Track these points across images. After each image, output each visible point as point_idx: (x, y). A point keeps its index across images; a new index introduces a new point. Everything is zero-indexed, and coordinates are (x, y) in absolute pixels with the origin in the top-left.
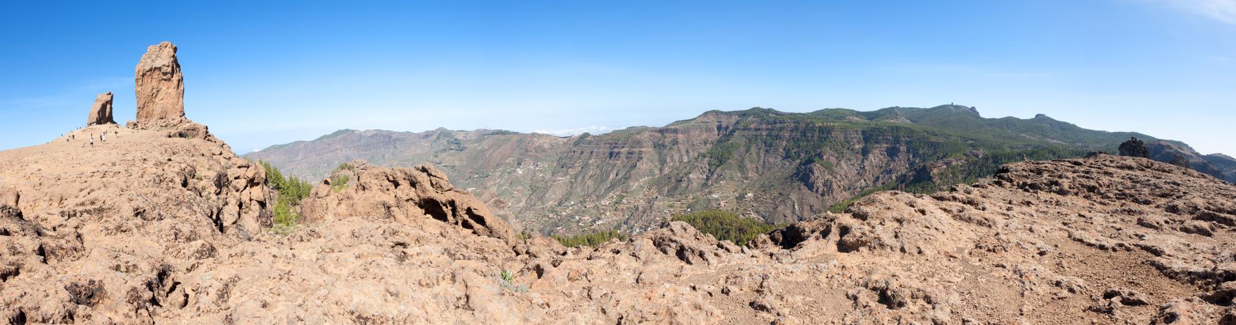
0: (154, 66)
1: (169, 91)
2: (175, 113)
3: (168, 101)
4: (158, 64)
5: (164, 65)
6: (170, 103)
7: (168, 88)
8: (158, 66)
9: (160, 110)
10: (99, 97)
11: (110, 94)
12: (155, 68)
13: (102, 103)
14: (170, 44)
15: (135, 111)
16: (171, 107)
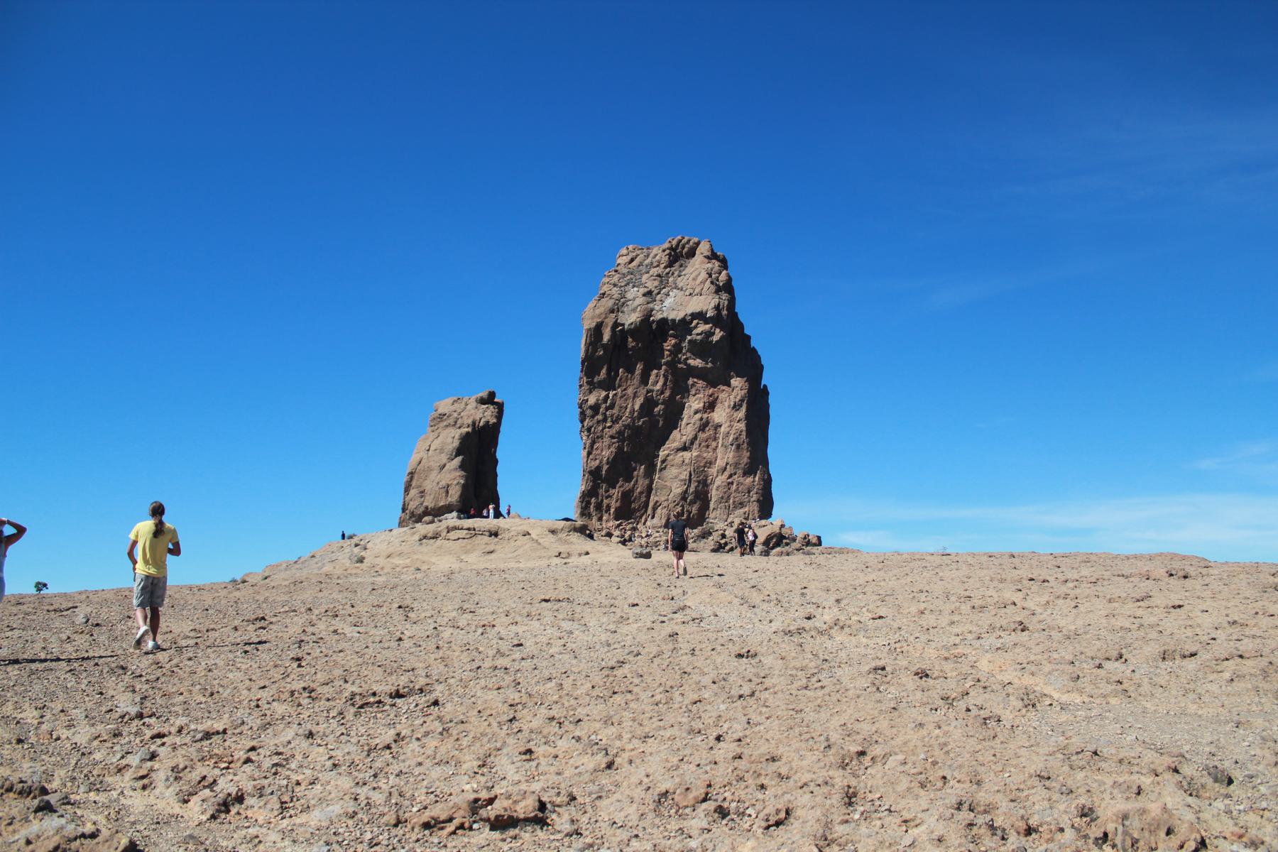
0: (658, 316)
1: (719, 415)
2: (742, 505)
3: (708, 455)
4: (673, 306)
5: (700, 316)
6: (720, 463)
7: (711, 406)
8: (677, 315)
9: (677, 489)
10: (445, 406)
11: (490, 399)
12: (664, 321)
13: (470, 429)
14: (704, 248)
15: (577, 485)
16: (720, 480)
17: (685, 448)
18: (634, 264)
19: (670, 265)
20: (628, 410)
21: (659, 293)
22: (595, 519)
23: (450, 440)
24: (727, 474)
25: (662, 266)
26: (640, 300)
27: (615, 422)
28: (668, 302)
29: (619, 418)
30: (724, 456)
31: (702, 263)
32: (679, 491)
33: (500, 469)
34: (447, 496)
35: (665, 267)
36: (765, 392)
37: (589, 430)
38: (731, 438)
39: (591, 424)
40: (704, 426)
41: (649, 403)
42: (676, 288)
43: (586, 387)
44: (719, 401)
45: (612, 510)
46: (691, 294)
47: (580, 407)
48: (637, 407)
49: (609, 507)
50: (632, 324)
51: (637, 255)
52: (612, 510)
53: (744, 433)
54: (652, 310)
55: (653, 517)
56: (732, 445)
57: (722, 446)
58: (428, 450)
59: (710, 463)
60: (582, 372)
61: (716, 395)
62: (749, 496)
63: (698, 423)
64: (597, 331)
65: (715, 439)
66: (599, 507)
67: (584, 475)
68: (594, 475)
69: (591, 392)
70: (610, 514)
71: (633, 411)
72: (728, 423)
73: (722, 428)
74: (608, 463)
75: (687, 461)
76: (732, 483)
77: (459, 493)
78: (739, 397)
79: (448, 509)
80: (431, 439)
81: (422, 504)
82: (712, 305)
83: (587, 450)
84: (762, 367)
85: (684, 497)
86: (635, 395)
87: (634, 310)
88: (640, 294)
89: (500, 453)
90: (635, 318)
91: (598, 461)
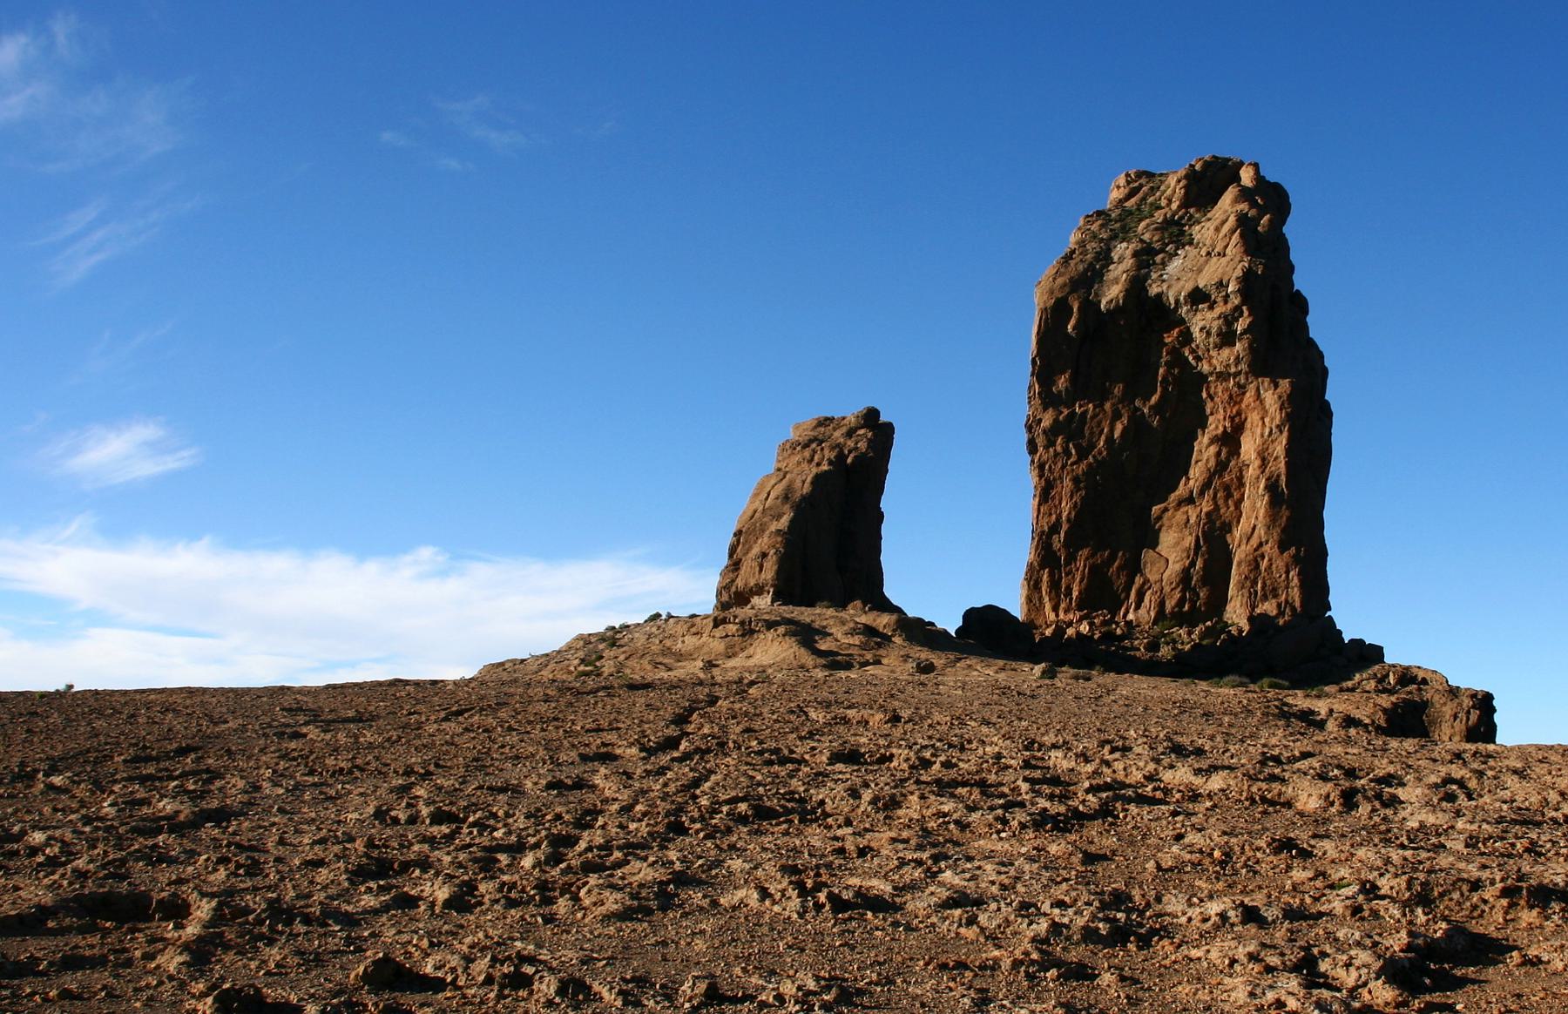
9: (1175, 567)
17: (1190, 500)
18: (1133, 201)
19: (1185, 204)
20: (1103, 437)
21: (1162, 251)
22: (1048, 607)
23: (798, 484)
24: (1254, 542)
25: (1174, 206)
26: (1129, 262)
27: (1082, 455)
28: (1175, 266)
29: (1092, 446)
30: (1254, 509)
31: (1236, 201)
32: (1178, 567)
33: (885, 529)
34: (761, 570)
35: (1180, 208)
36: (1325, 413)
37: (1041, 467)
38: (1262, 486)
39: (1045, 457)
40: (1221, 466)
41: (1137, 425)
42: (1191, 243)
43: (1038, 401)
44: (1248, 425)
45: (1075, 594)
46: (1209, 254)
47: (1029, 428)
48: (1117, 434)
49: (1069, 590)
50: (1112, 300)
51: (1141, 186)
52: (1075, 594)
53: (1283, 478)
54: (1148, 276)
55: (1138, 607)
56: (1264, 495)
57: (1249, 497)
58: (767, 499)
59: (1227, 528)
60: (1032, 375)
61: (1243, 416)
62: (1287, 577)
63: (1212, 463)
64: (1054, 316)
65: (1241, 484)
66: (1054, 585)
67: (1033, 538)
68: (1043, 542)
69: (1045, 409)
70: (1071, 599)
71: (1110, 439)
72: (1258, 463)
73: (1251, 467)
74: (1069, 520)
75: (1193, 520)
76: (1263, 557)
77: (775, 567)
78: (1277, 421)
79: (759, 590)
80: (773, 482)
81: (733, 581)
82: (1239, 273)
83: (1037, 500)
84: (1325, 372)
85: (1185, 577)
86: (1117, 416)
87: (1116, 281)
88: (1128, 253)
89: (888, 503)
90: (1116, 292)
91: (1054, 517)
